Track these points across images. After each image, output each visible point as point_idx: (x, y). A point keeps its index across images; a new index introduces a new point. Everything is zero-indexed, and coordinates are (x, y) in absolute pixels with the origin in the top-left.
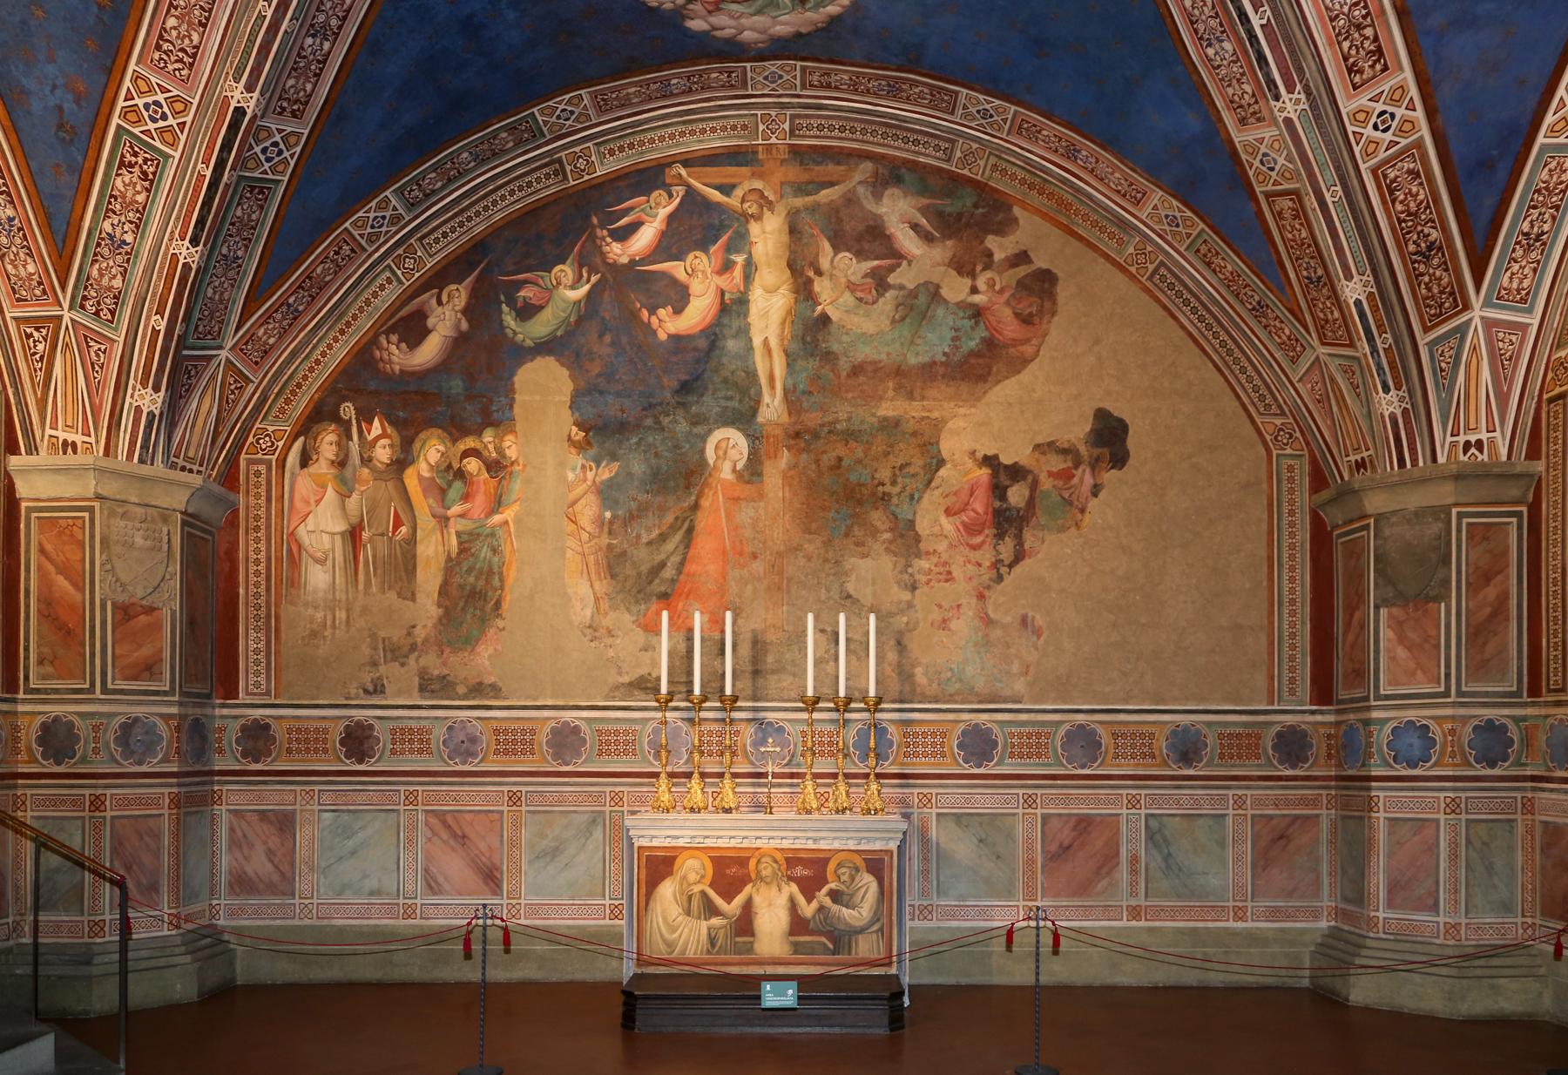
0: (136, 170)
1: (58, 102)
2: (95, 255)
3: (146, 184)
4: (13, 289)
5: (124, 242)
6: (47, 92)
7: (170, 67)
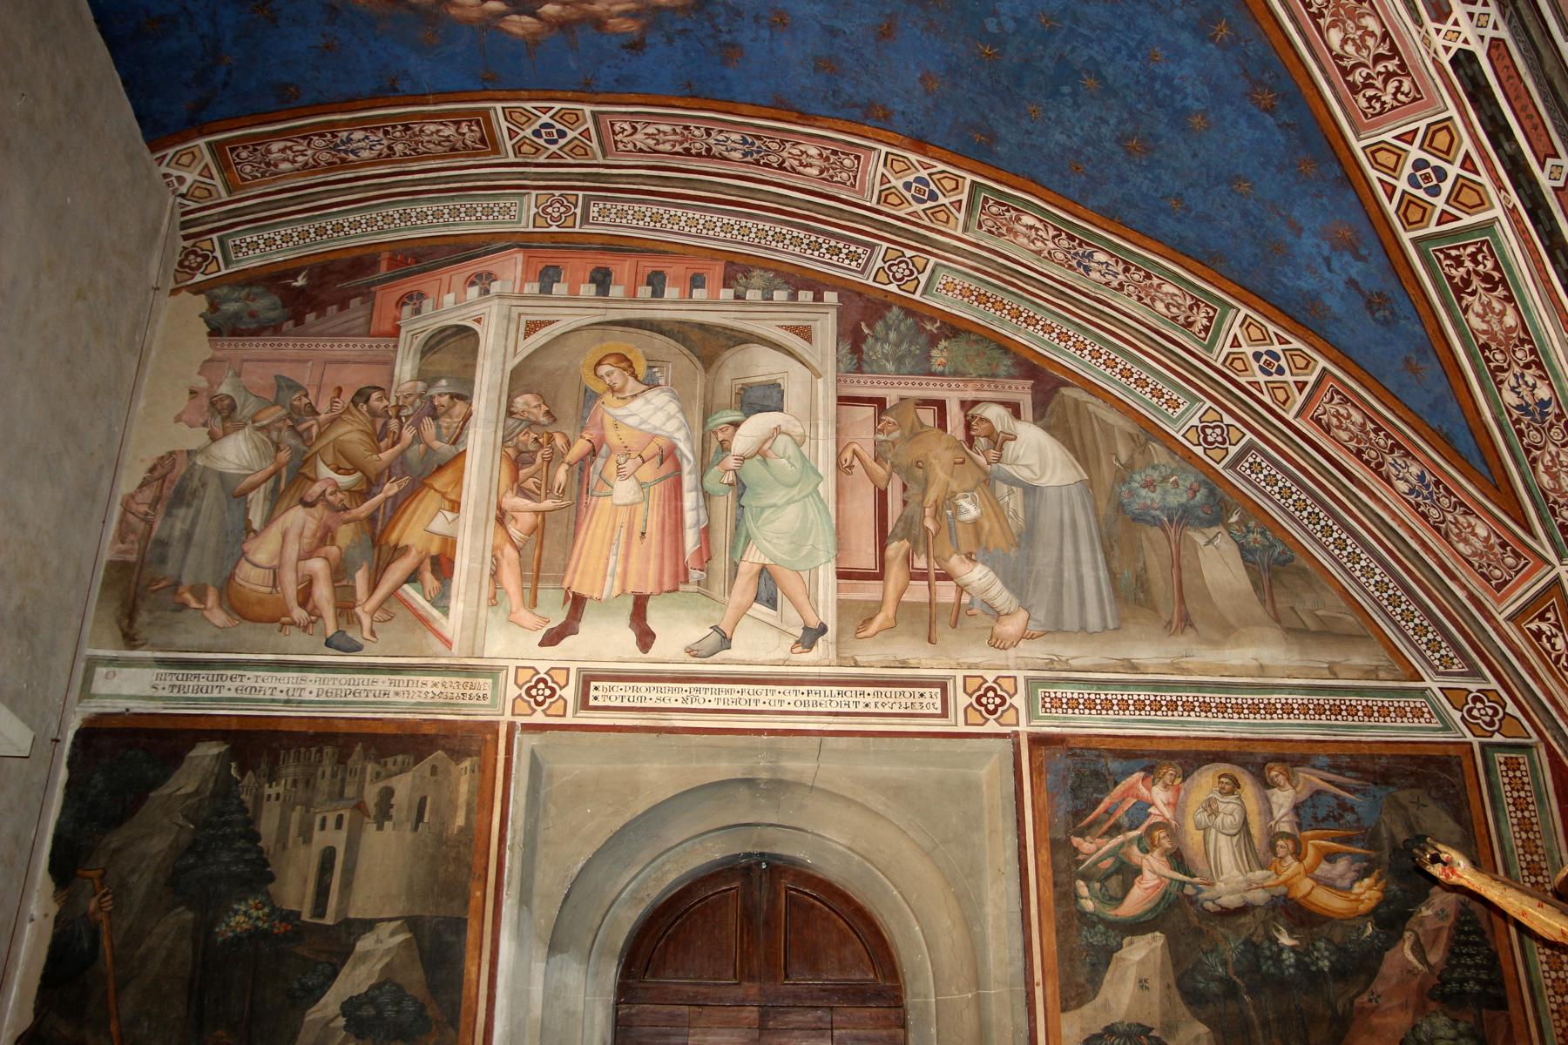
0: (1476, 283)
1: (1344, 276)
2: (1528, 452)
3: (1500, 292)
4: (1483, 575)
5: (1544, 404)
6: (1327, 275)
7: (1387, 98)
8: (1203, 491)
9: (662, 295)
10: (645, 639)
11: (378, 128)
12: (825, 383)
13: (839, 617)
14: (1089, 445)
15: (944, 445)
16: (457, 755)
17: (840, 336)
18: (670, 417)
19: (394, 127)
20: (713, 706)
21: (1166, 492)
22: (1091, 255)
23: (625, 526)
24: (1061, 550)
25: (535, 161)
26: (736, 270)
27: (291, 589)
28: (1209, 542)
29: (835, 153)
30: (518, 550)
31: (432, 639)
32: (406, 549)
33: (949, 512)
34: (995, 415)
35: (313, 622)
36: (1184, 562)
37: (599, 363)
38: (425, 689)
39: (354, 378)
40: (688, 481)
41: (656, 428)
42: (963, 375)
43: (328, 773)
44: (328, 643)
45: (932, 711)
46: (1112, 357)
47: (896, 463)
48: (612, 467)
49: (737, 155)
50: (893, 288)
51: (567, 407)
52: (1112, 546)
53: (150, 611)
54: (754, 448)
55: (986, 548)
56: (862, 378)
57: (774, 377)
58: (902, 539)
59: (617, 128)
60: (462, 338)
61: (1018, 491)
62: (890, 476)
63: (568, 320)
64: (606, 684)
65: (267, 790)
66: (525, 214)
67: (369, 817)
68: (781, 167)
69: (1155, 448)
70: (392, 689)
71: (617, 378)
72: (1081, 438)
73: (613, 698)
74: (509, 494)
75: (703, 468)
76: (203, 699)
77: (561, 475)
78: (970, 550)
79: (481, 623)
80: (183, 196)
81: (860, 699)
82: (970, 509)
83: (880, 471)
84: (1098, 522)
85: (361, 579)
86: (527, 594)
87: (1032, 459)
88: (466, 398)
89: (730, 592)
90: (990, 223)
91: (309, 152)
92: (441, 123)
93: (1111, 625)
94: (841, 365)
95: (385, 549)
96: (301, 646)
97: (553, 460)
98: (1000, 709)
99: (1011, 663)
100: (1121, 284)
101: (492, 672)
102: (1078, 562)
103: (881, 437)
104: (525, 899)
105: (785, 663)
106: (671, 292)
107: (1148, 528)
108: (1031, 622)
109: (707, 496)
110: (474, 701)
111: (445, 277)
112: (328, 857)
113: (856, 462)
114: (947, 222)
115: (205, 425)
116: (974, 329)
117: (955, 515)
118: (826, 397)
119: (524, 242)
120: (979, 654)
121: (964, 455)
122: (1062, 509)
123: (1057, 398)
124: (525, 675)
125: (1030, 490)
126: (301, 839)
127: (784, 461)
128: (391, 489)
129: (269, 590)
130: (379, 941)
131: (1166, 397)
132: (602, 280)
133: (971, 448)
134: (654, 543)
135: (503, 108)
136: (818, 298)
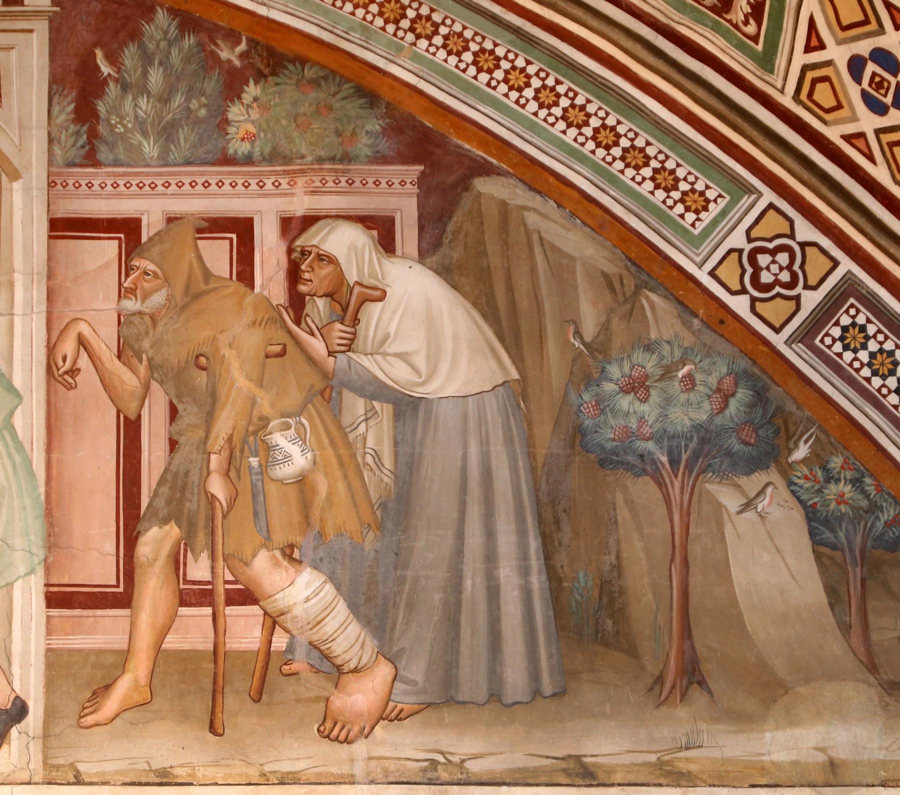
8: (743, 394)
12: (27, 191)
13: (50, 685)
14: (524, 304)
15: (248, 316)
17: (56, 81)
21: (668, 401)
24: (460, 535)
28: (748, 505)
33: (254, 461)
36: (695, 551)
42: (287, 160)
46: (580, 101)
47: (158, 360)
52: (557, 522)
55: (321, 534)
56: (98, 176)
58: (165, 521)
61: (384, 410)
62: (147, 388)
72: (510, 289)
78: (292, 539)
84: (533, 470)
93: (548, 688)
94: (57, 150)
99: (359, 770)
102: (491, 558)
103: (131, 305)
107: (629, 480)
108: (397, 685)
113: (84, 362)
116: (314, 54)
117: (265, 467)
118: (28, 221)
121: (283, 337)
122: (465, 446)
123: (467, 200)
131: (684, 186)
133: (298, 322)
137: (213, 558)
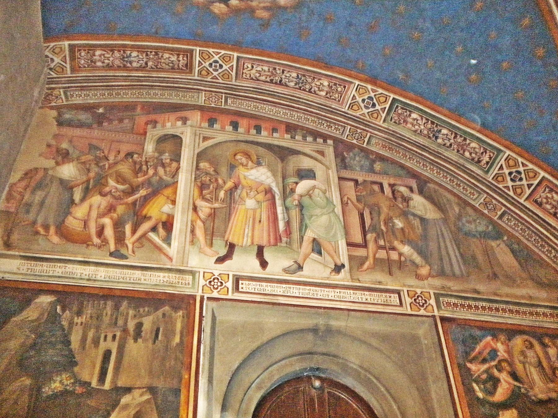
9: (260, 133)
10: (264, 264)
11: (144, 52)
12: (332, 171)
13: (350, 262)
16: (176, 309)
18: (268, 178)
19: (151, 52)
20: (297, 295)
22: (440, 131)
23: (252, 217)
25: (205, 79)
26: (291, 128)
27: (93, 230)
29: (335, 84)
30: (204, 223)
31: (163, 257)
32: (150, 218)
33: (391, 224)
34: (403, 189)
35: (103, 245)
37: (235, 155)
38: (159, 279)
39: (125, 148)
40: (278, 202)
41: (262, 181)
43: (109, 313)
44: (111, 254)
45: (395, 304)
48: (244, 194)
49: (292, 84)
50: (355, 141)
51: (224, 170)
53: (18, 234)
54: (305, 192)
57: (310, 168)
58: (372, 233)
59: (245, 66)
60: (177, 140)
61: (418, 220)
63: (220, 138)
64: (247, 282)
65: (76, 320)
66: (201, 100)
67: (130, 336)
68: (310, 91)
69: (469, 210)
70: (142, 277)
71: (244, 160)
73: (250, 289)
74: (198, 200)
75: (285, 197)
76: (44, 276)
77: (222, 194)
79: (186, 252)
80: (51, 69)
81: (363, 296)
82: (399, 224)
83: (360, 206)
85: (128, 228)
86: (208, 241)
87: (421, 208)
88: (178, 160)
89: (300, 248)
90: (396, 118)
91: (111, 59)
92: (172, 54)
95: (140, 217)
96: (96, 256)
97: (218, 188)
98: (425, 305)
100: (451, 145)
101: (192, 273)
104: (210, 380)
105: (328, 278)
106: (264, 133)
109: (287, 209)
110: (184, 286)
111: (167, 116)
112: (107, 355)
114: (377, 118)
115: (53, 159)
117: (393, 226)
119: (201, 108)
120: (412, 281)
124: (208, 276)
125: (422, 220)
126: (93, 345)
127: (318, 198)
128: (143, 192)
129: (81, 229)
130: (133, 399)
132: (235, 126)
134: (265, 225)
135: (200, 50)
136: (325, 141)
137: (384, 241)
